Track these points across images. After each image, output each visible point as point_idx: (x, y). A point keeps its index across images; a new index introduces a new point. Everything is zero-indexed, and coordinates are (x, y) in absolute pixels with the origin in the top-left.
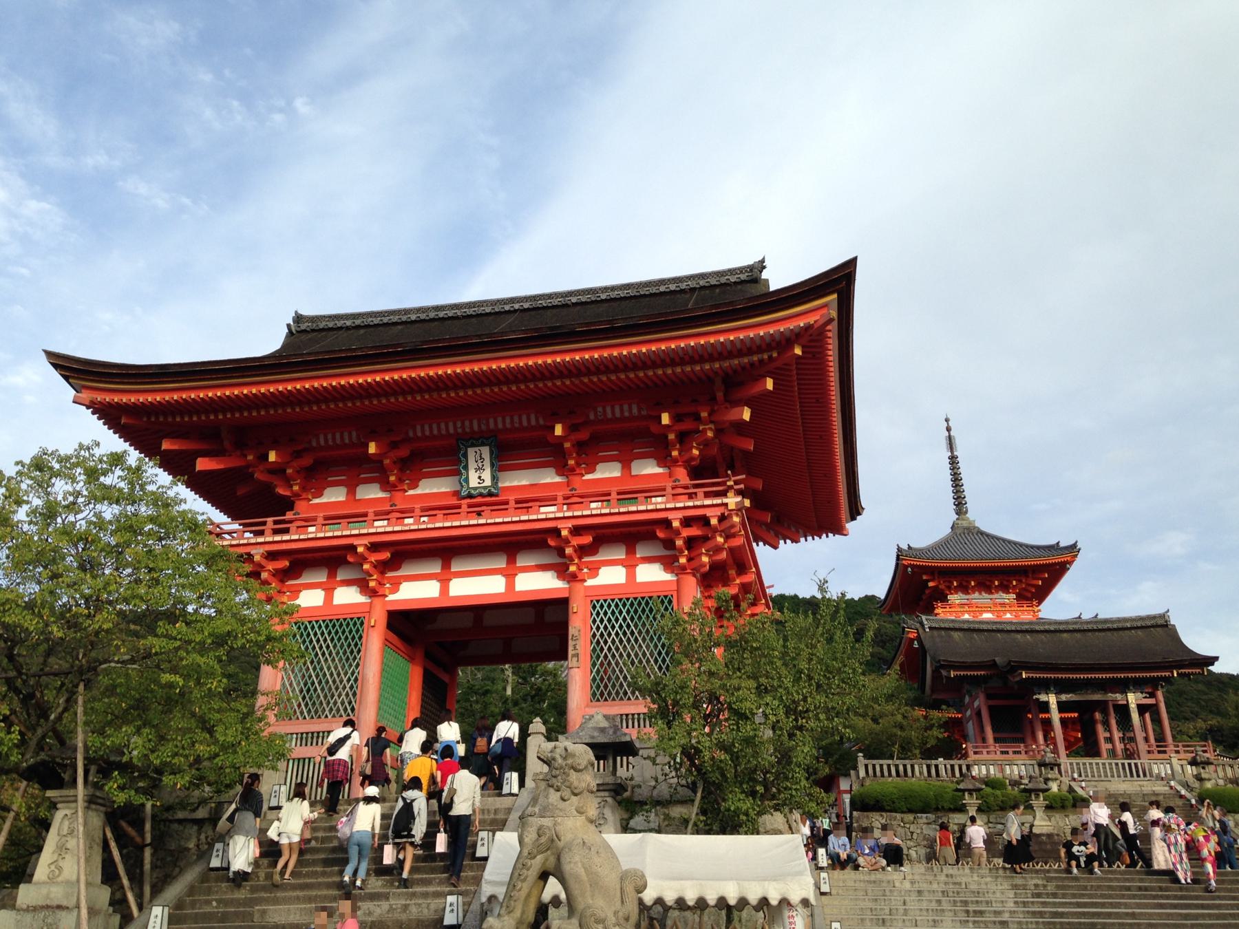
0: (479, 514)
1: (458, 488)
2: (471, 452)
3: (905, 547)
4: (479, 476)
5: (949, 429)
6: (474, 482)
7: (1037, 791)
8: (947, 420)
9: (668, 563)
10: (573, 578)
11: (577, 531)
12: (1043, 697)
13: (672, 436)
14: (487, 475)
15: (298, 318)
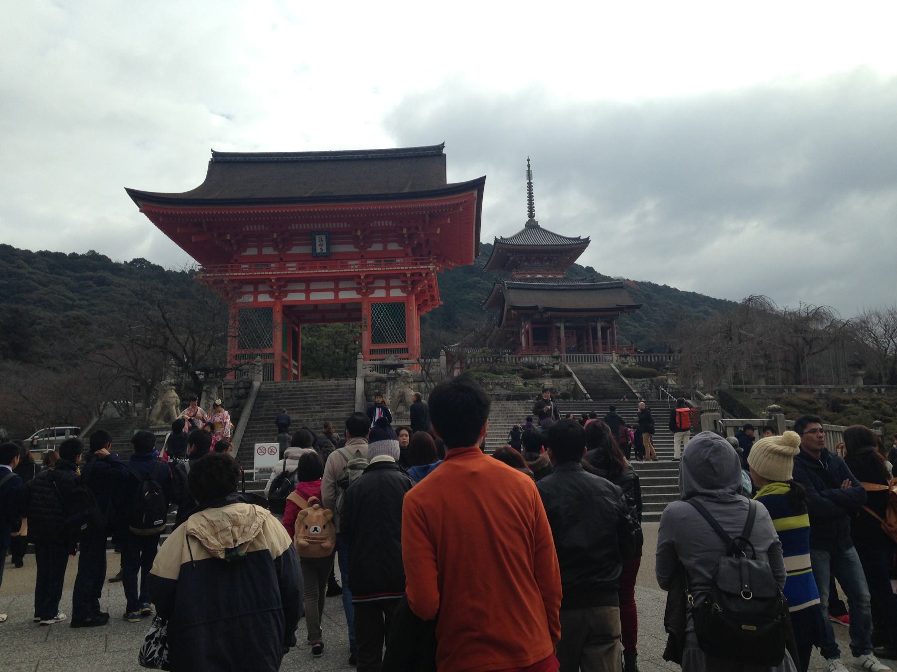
0: (325, 268)
1: (311, 251)
2: (317, 237)
3: (499, 238)
4: (321, 247)
5: (529, 166)
6: (318, 250)
7: (548, 370)
8: (528, 160)
9: (403, 289)
10: (365, 295)
11: (367, 276)
12: (558, 325)
13: (406, 236)
14: (324, 248)
15: (215, 154)
